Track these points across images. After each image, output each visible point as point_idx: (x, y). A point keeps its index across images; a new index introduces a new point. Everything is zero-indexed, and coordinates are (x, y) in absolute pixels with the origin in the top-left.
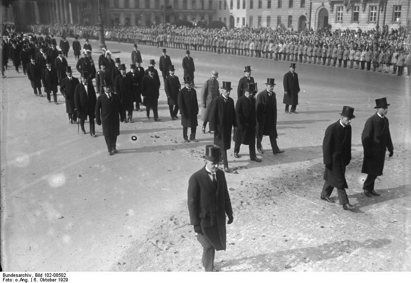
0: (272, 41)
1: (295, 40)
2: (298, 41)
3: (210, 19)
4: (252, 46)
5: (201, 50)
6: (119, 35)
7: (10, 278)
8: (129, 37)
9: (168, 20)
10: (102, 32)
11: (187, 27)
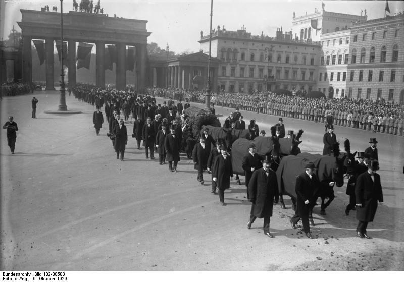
0: (371, 114)
1: (396, 114)
2: (398, 115)
3: (310, 89)
4: (351, 117)
6: (223, 100)
7: (10, 277)
8: (232, 103)
9: (269, 88)
10: (209, 97)
11: (287, 96)
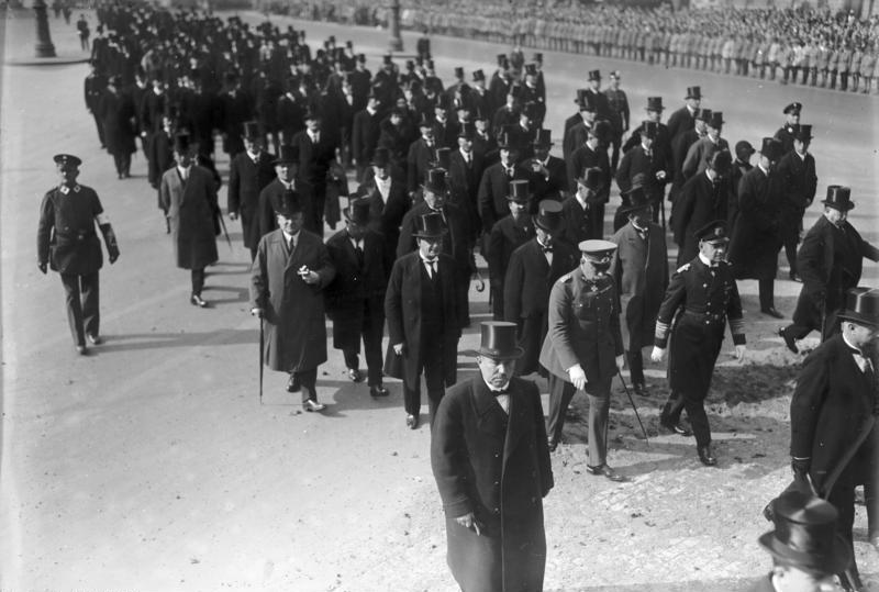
0: (776, 40)
1: (833, 39)
2: (840, 40)
4: (729, 50)
5: (610, 55)
6: (432, 18)
